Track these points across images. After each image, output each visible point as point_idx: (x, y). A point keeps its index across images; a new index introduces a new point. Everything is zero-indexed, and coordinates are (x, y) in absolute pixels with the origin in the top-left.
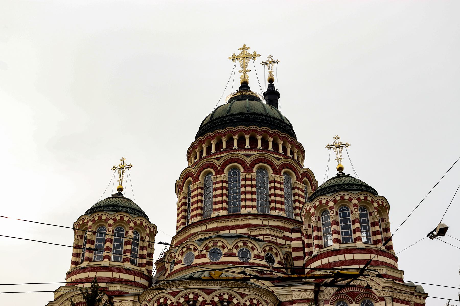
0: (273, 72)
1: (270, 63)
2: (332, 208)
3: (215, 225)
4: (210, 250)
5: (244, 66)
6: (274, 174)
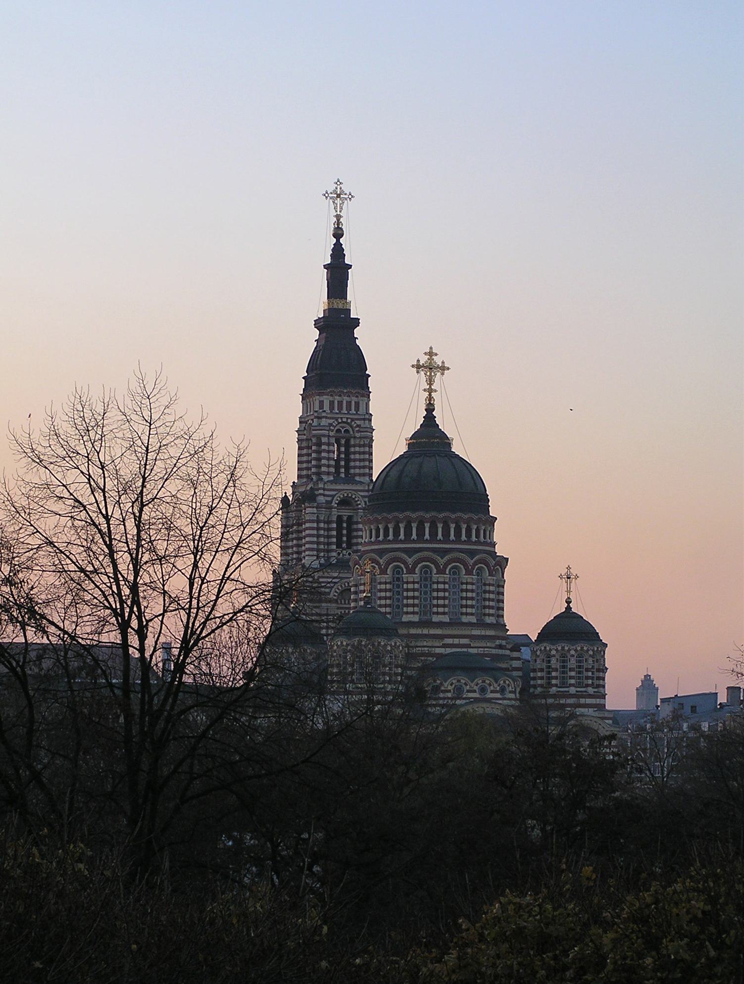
0: (341, 217)
1: (339, 196)
2: (573, 656)
3: (438, 632)
4: (479, 686)
5: (430, 382)
6: (489, 576)
